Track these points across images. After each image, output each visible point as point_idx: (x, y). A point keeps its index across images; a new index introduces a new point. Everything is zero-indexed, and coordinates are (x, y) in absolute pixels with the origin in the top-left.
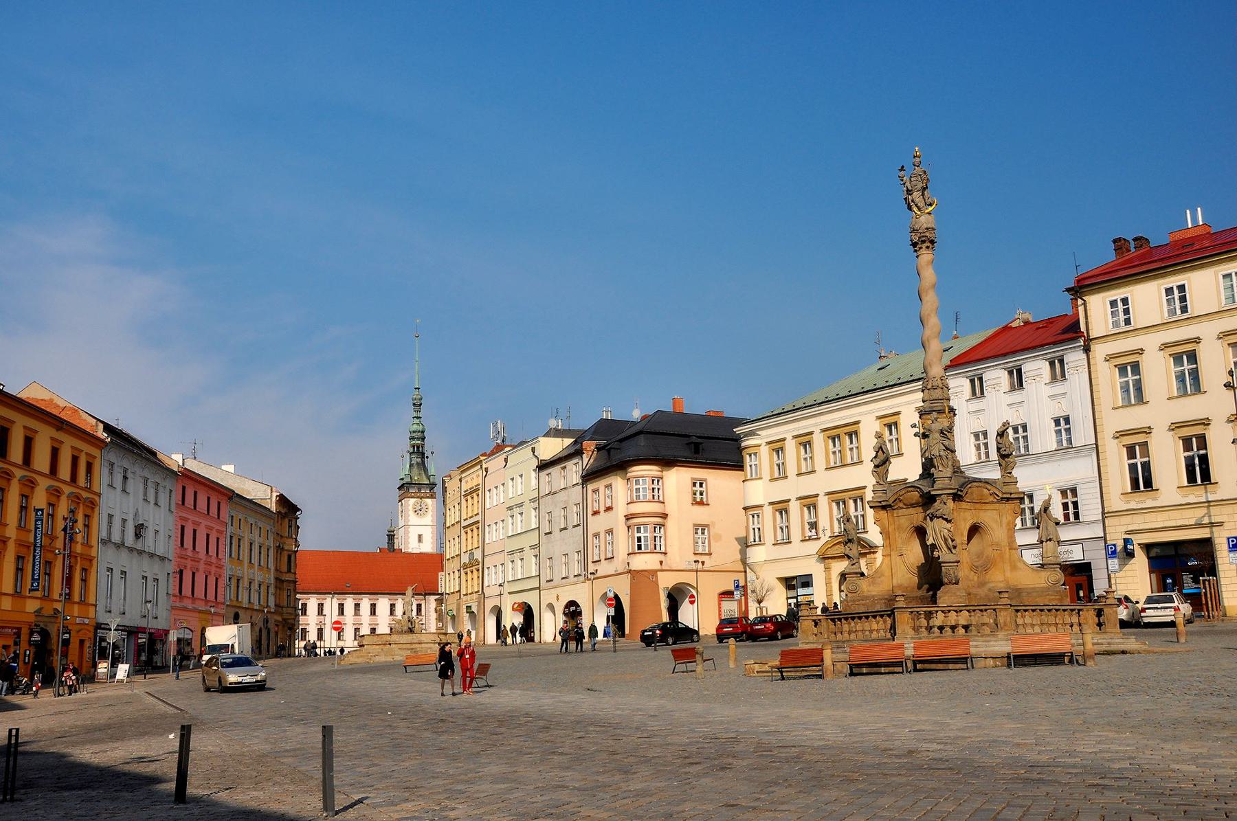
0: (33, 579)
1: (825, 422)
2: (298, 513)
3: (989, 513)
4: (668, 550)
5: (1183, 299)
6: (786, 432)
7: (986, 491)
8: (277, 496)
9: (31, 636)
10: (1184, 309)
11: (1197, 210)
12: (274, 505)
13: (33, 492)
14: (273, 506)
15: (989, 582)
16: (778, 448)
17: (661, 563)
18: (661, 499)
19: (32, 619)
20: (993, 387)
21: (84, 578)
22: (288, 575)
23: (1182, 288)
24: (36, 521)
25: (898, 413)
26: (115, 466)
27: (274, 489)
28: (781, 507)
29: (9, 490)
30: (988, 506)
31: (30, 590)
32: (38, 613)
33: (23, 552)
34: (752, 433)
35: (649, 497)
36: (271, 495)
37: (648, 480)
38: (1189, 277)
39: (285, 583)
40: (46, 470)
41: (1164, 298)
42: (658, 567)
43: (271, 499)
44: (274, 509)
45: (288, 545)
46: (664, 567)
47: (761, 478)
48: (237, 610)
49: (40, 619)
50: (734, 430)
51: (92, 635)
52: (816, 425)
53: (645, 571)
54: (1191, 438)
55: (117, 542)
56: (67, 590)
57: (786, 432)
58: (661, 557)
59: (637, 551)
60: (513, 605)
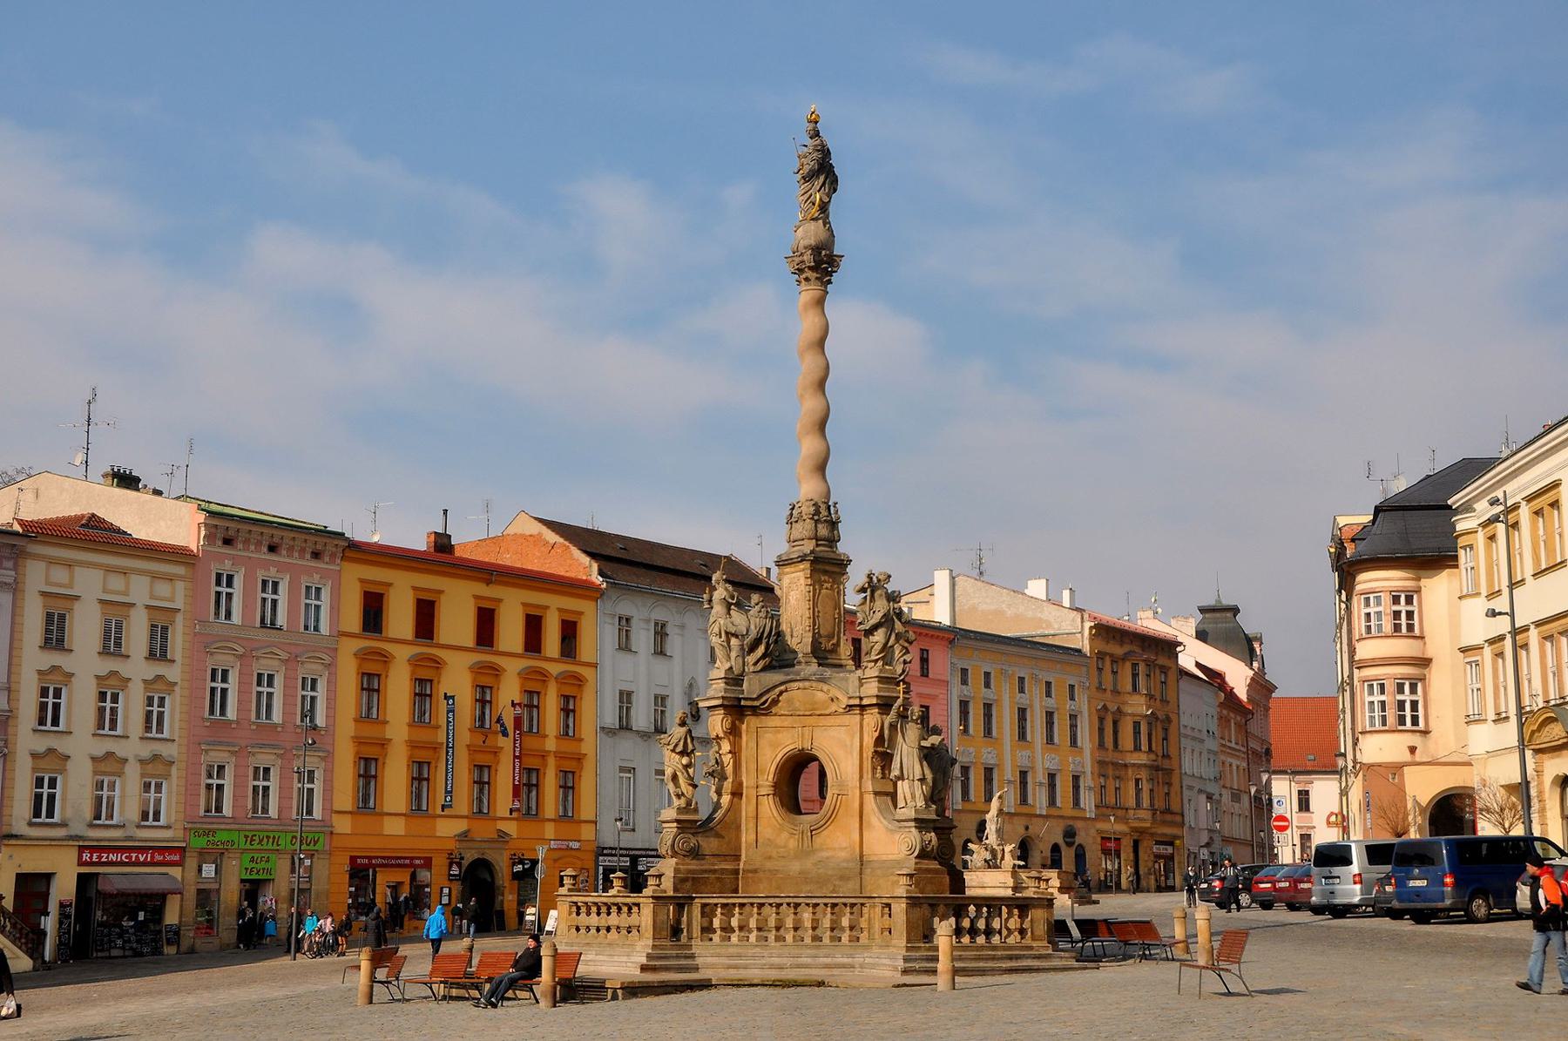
0: (447, 792)
2: (1179, 649)
3: (833, 732)
4: (1433, 725)
7: (820, 694)
8: (1091, 628)
9: (450, 870)
12: (1086, 642)
13: (439, 675)
14: (1084, 643)
15: (822, 850)
17: (1413, 750)
18: (1417, 632)
19: (451, 845)
21: (449, 789)
22: (1136, 755)
24: (448, 712)
26: (634, 622)
27: (1086, 616)
29: (387, 676)
30: (831, 720)
31: (443, 808)
32: (464, 837)
33: (423, 755)
35: (1388, 627)
36: (1082, 626)
37: (1386, 599)
39: (1130, 771)
40: (468, 638)
42: (1407, 757)
43: (1081, 632)
44: (1087, 649)
45: (1132, 705)
46: (1418, 757)
49: (465, 844)
50: (1449, 502)
51: (591, 865)
53: (1380, 765)
55: (641, 729)
56: (517, 803)
58: (1415, 740)
59: (1368, 729)
60: (1329, 817)
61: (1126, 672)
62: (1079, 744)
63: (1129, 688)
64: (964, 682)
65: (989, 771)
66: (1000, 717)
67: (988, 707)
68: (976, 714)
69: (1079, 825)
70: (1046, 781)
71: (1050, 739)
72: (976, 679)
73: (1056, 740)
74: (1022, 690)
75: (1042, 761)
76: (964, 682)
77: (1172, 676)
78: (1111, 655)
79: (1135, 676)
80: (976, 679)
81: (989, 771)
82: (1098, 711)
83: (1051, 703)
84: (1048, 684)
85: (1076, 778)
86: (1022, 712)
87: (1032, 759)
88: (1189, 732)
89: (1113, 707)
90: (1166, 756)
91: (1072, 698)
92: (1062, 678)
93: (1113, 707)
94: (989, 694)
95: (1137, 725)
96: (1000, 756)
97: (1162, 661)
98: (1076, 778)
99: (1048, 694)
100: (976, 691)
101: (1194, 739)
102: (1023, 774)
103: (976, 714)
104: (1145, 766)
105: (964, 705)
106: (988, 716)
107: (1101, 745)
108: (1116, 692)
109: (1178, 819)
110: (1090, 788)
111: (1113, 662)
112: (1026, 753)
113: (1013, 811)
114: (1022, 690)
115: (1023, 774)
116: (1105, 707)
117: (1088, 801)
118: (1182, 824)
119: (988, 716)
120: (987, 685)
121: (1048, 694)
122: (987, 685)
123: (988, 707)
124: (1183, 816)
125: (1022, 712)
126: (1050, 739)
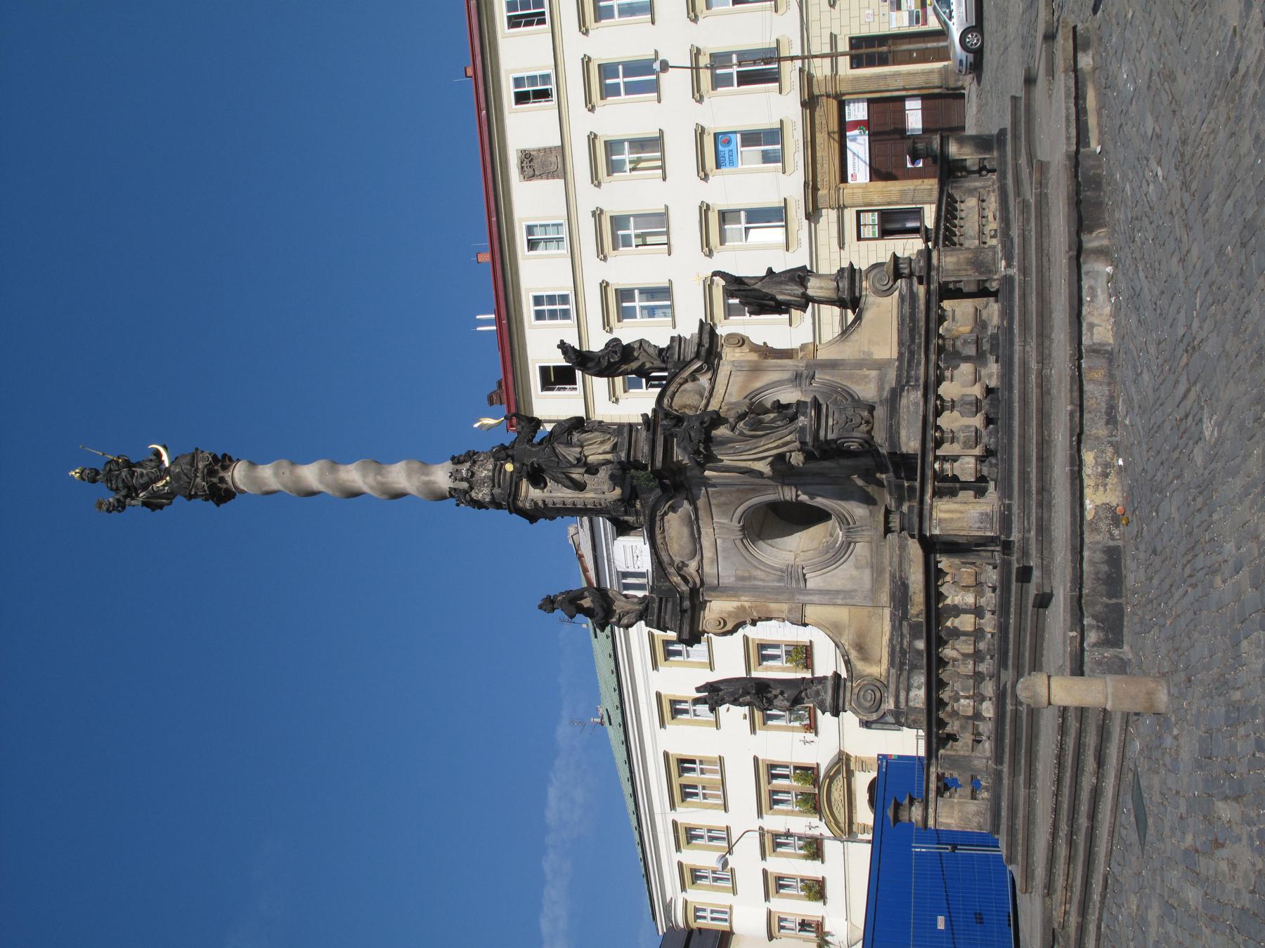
1: (662, 805)
5: (551, 299)
6: (670, 859)
10: (564, 299)
11: (479, 320)
16: (692, 876)
20: (635, 558)
23: (538, 300)
25: (659, 696)
28: (775, 884)
34: (668, 908)
38: (526, 289)
41: (547, 322)
47: (731, 908)
52: (663, 813)
54: (729, 304)
57: (670, 859)
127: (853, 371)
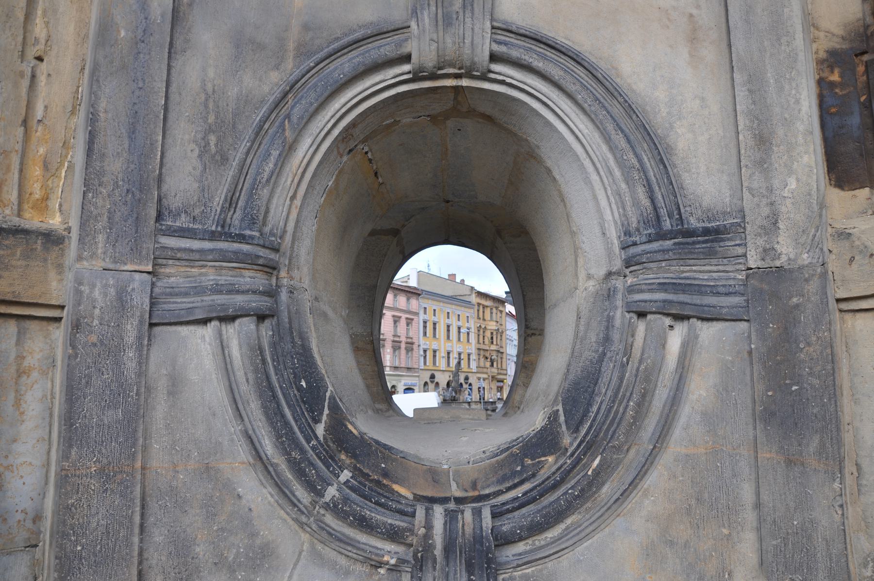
45: (490, 325)
48: (433, 372)
61: (488, 311)
62: (470, 341)
63: (489, 319)
64: (425, 313)
65: (435, 351)
66: (440, 329)
67: (435, 324)
68: (430, 326)
69: (470, 375)
70: (457, 356)
71: (459, 339)
72: (430, 311)
73: (462, 340)
74: (448, 318)
75: (456, 348)
76: (425, 313)
77: (504, 314)
78: (483, 305)
79: (491, 313)
80: (430, 311)
81: (435, 351)
82: (478, 327)
83: (460, 324)
84: (459, 315)
85: (469, 355)
86: (448, 326)
87: (452, 347)
88: (509, 337)
89: (483, 326)
90: (502, 347)
91: (468, 322)
92: (464, 312)
93: (483, 326)
94: (436, 319)
95: (492, 333)
96: (439, 345)
97: (501, 308)
98: (469, 355)
99: (459, 320)
100: (430, 317)
101: (510, 340)
102: (449, 353)
103: (430, 326)
104: (495, 350)
105: (425, 322)
106: (435, 329)
107: (478, 342)
108: (484, 320)
109: (505, 372)
110: (475, 360)
111: (483, 308)
112: (450, 344)
113: (444, 369)
114: (448, 318)
115: (449, 353)
116: (480, 326)
117: (473, 365)
118: (506, 374)
119: (435, 329)
120: (434, 315)
121: (459, 320)
122: (434, 315)
123: (435, 324)
124: (506, 370)
125: (448, 326)
126: (459, 339)
127: (750, 516)
